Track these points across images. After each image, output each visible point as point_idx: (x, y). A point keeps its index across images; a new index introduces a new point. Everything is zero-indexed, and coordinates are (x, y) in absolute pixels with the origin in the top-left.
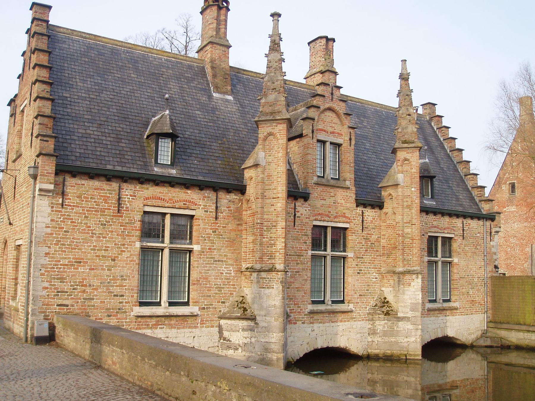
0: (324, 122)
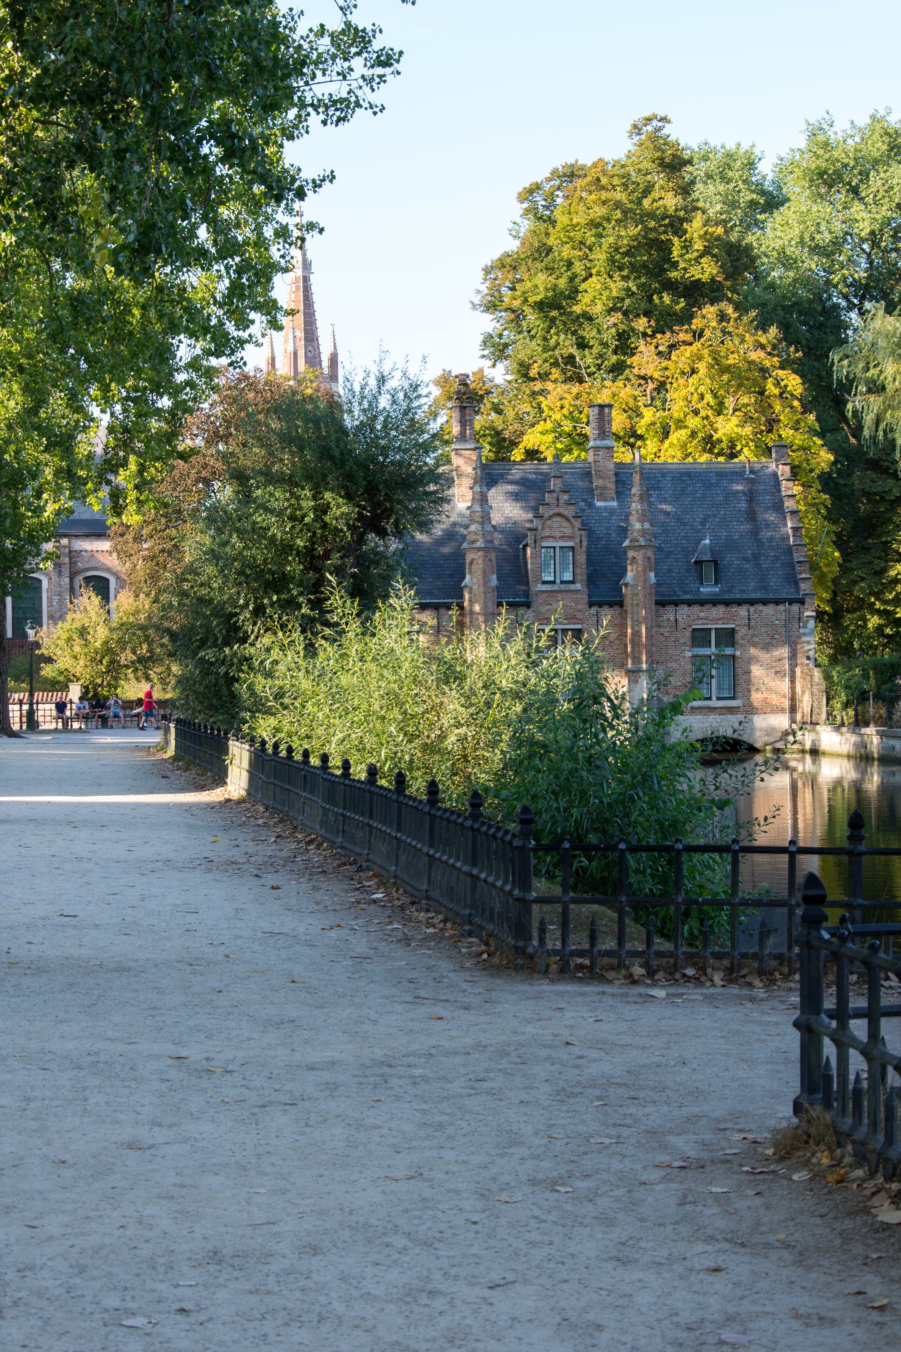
0: (550, 528)
